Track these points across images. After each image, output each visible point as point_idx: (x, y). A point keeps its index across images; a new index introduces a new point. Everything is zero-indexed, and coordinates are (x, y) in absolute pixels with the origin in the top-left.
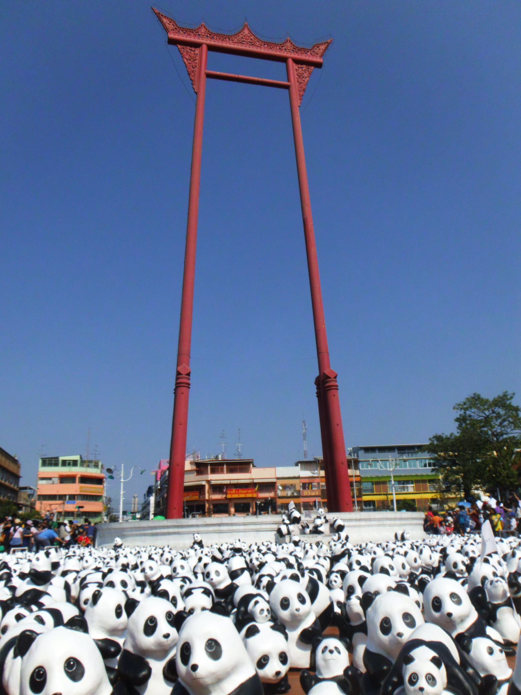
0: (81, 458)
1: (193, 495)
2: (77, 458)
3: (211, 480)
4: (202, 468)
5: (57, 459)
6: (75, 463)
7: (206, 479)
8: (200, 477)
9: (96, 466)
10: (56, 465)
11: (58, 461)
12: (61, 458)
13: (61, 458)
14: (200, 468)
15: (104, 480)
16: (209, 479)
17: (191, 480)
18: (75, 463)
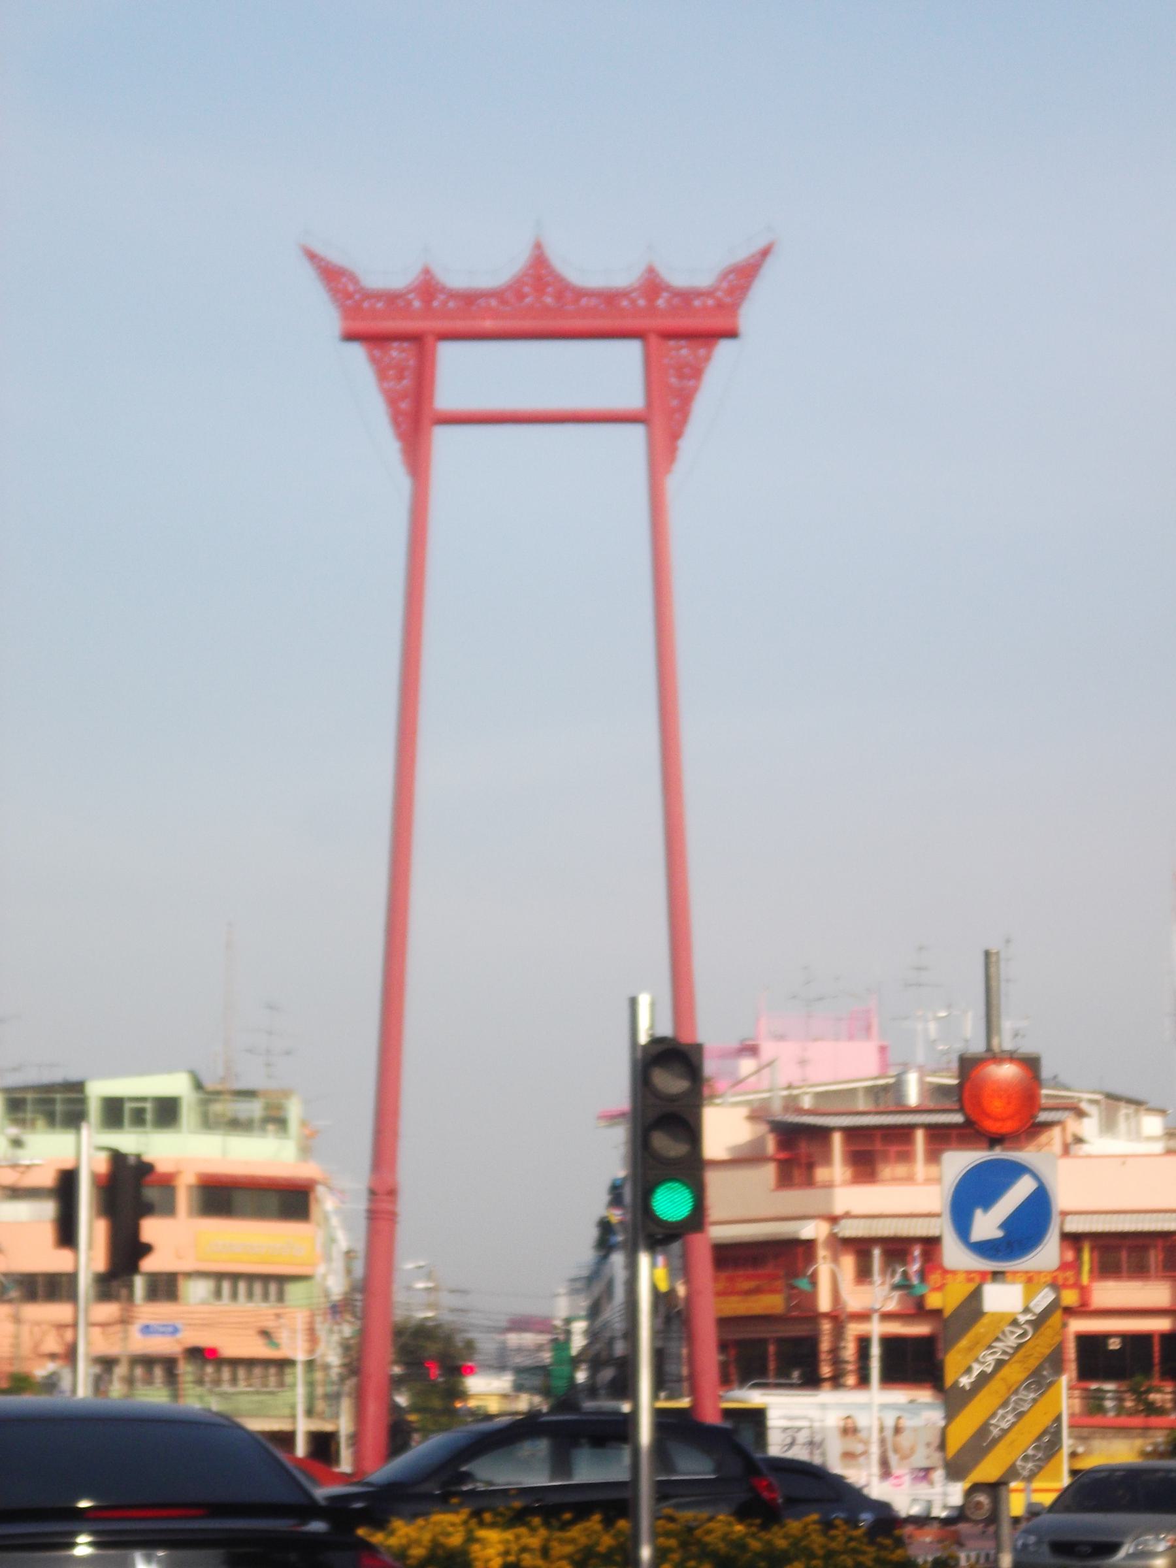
0: (198, 1086)
1: (757, 1291)
2: (176, 1085)
3: (847, 1215)
4: (804, 1147)
5: (76, 1088)
6: (166, 1112)
7: (821, 1209)
8: (795, 1199)
9: (276, 1120)
10: (74, 1118)
11: (83, 1101)
12: (98, 1089)
13: (98, 1089)
14: (795, 1145)
15: (320, 1191)
16: (838, 1210)
17: (743, 1206)
18: (166, 1112)
